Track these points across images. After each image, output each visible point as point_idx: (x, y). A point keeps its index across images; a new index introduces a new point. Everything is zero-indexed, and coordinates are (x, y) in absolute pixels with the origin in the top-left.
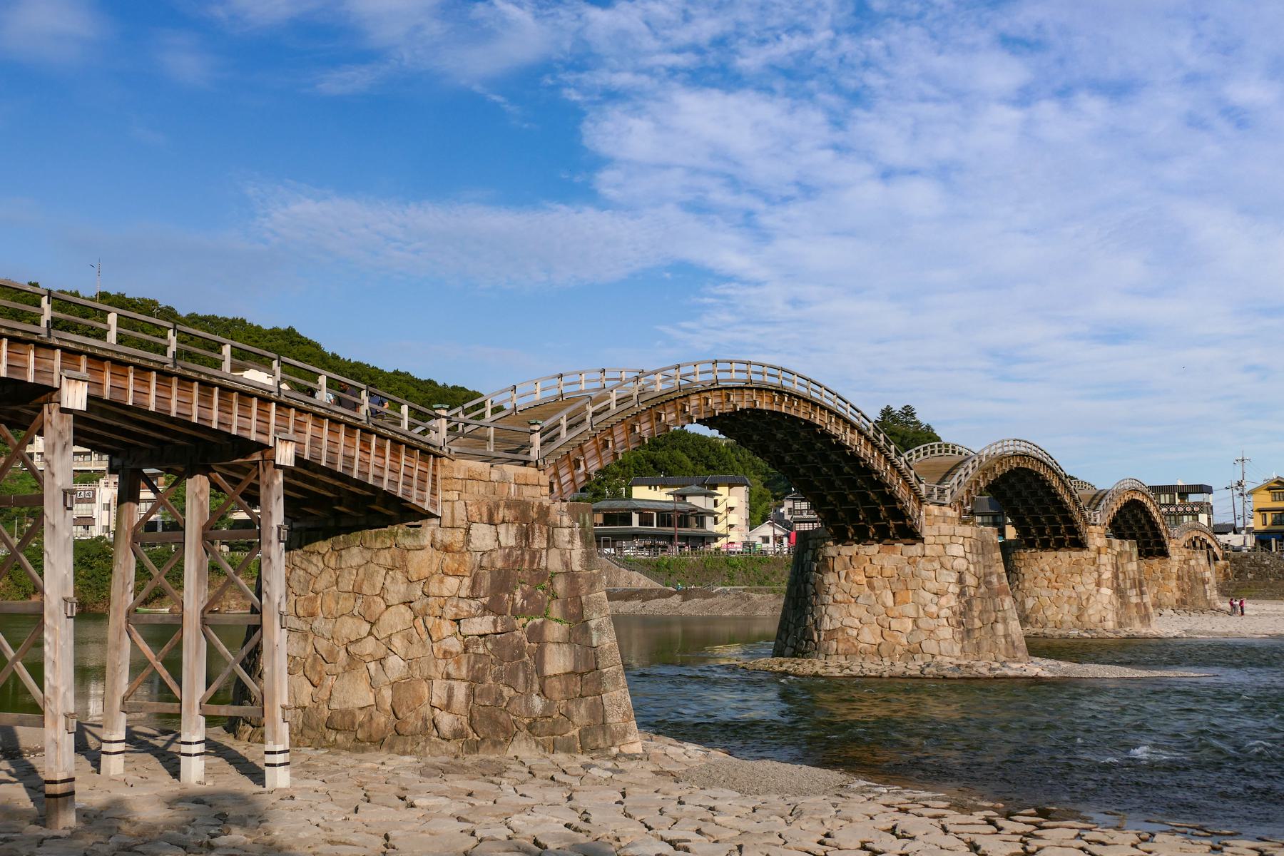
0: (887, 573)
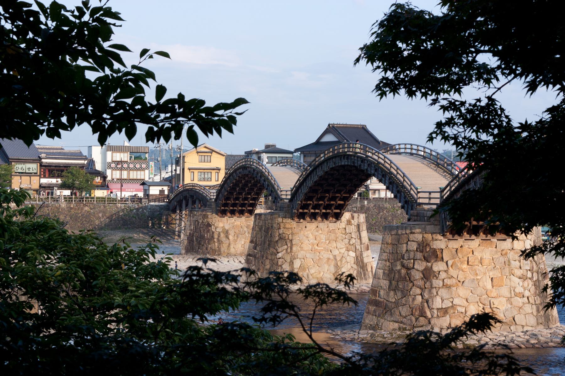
0: (486, 262)
